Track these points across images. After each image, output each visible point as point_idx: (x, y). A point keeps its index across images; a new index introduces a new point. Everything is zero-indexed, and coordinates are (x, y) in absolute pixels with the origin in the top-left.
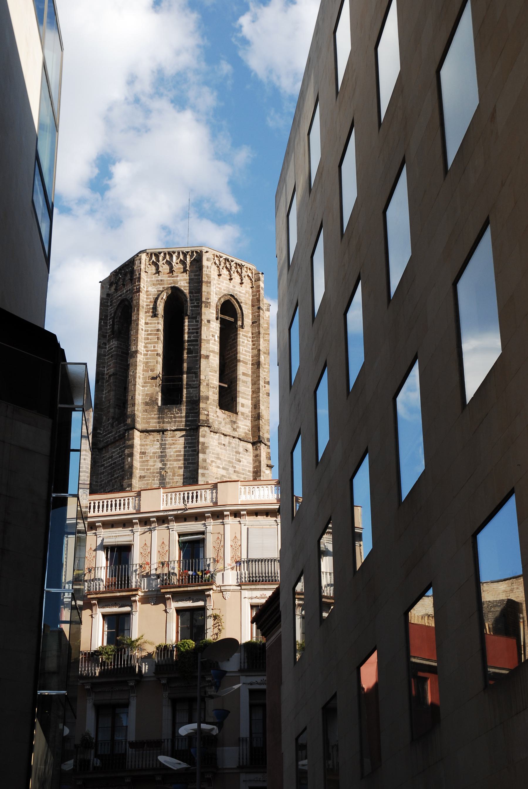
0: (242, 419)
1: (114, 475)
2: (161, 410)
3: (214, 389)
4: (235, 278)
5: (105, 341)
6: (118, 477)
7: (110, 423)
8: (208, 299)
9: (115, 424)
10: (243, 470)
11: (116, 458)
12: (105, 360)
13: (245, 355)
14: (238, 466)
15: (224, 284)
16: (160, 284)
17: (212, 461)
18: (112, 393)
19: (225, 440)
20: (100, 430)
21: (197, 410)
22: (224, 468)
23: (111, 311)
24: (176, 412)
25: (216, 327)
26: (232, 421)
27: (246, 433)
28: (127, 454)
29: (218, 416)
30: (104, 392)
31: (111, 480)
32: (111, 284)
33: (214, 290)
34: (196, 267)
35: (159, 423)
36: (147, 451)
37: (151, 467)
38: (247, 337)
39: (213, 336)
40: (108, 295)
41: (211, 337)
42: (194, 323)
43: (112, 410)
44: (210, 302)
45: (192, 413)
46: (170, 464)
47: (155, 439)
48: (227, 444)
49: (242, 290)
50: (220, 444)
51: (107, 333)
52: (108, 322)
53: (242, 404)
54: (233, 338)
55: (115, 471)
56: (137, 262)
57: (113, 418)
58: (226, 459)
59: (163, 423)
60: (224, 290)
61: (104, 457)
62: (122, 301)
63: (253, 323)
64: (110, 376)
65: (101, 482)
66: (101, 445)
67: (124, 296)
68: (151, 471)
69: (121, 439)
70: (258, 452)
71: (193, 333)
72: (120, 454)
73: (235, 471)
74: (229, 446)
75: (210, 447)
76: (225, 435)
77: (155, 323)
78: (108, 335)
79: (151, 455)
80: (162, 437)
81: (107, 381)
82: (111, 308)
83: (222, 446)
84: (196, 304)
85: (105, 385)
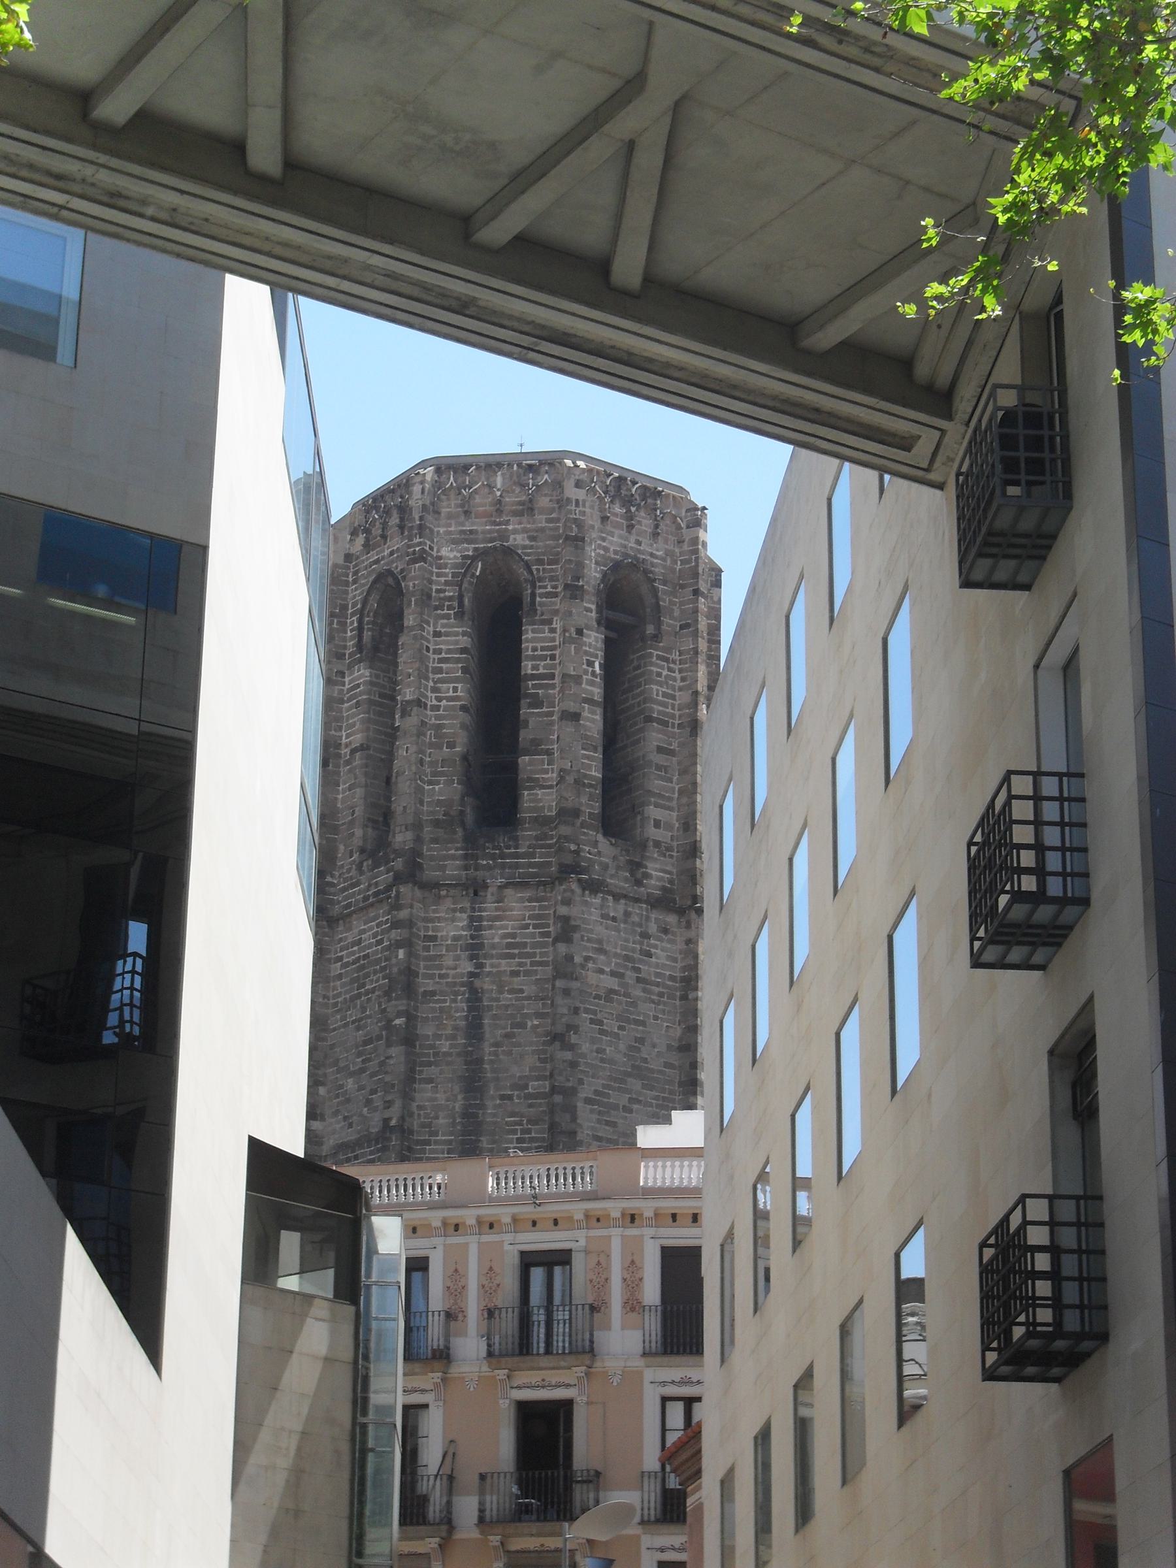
0: (656, 855)
1: (363, 985)
2: (470, 841)
3: (592, 790)
4: (639, 523)
5: (341, 668)
6: (373, 991)
7: (354, 861)
8: (578, 579)
9: (365, 864)
10: (658, 975)
11: (370, 946)
12: (341, 712)
13: (665, 705)
14: (646, 968)
15: (615, 539)
16: (470, 542)
17: (587, 959)
18: (359, 792)
19: (617, 909)
20: (332, 876)
21: (552, 839)
22: (613, 974)
23: (355, 597)
24: (504, 842)
25: (597, 642)
26: (631, 862)
27: (664, 889)
28: (397, 940)
29: (599, 852)
30: (340, 788)
31: (359, 996)
32: (354, 533)
33: (593, 554)
34: (551, 501)
35: (466, 868)
36: (439, 934)
37: (449, 971)
38: (666, 660)
39: (590, 664)
40: (348, 557)
41: (585, 666)
42: (547, 634)
43: (359, 832)
44: (583, 586)
45: (542, 847)
46: (492, 966)
47: (459, 906)
48: (620, 914)
49: (657, 550)
50: (604, 916)
51: (345, 647)
52: (348, 621)
53: (655, 820)
54: (636, 663)
55: (367, 975)
56: (417, 489)
57: (362, 851)
58: (619, 951)
59: (477, 868)
60: (616, 552)
61: (341, 940)
62: (380, 577)
63: (682, 628)
64: (353, 751)
65: (335, 997)
66: (336, 910)
67: (384, 565)
68: (449, 980)
69: (381, 901)
70: (691, 934)
71: (544, 658)
72: (379, 937)
73: (639, 980)
74: (625, 922)
75: (583, 926)
76: (617, 897)
77: (457, 634)
78: (347, 652)
79: (449, 942)
80: (473, 902)
81: (348, 762)
82: (356, 589)
83: (610, 922)
84: (549, 589)
85: (344, 770)
